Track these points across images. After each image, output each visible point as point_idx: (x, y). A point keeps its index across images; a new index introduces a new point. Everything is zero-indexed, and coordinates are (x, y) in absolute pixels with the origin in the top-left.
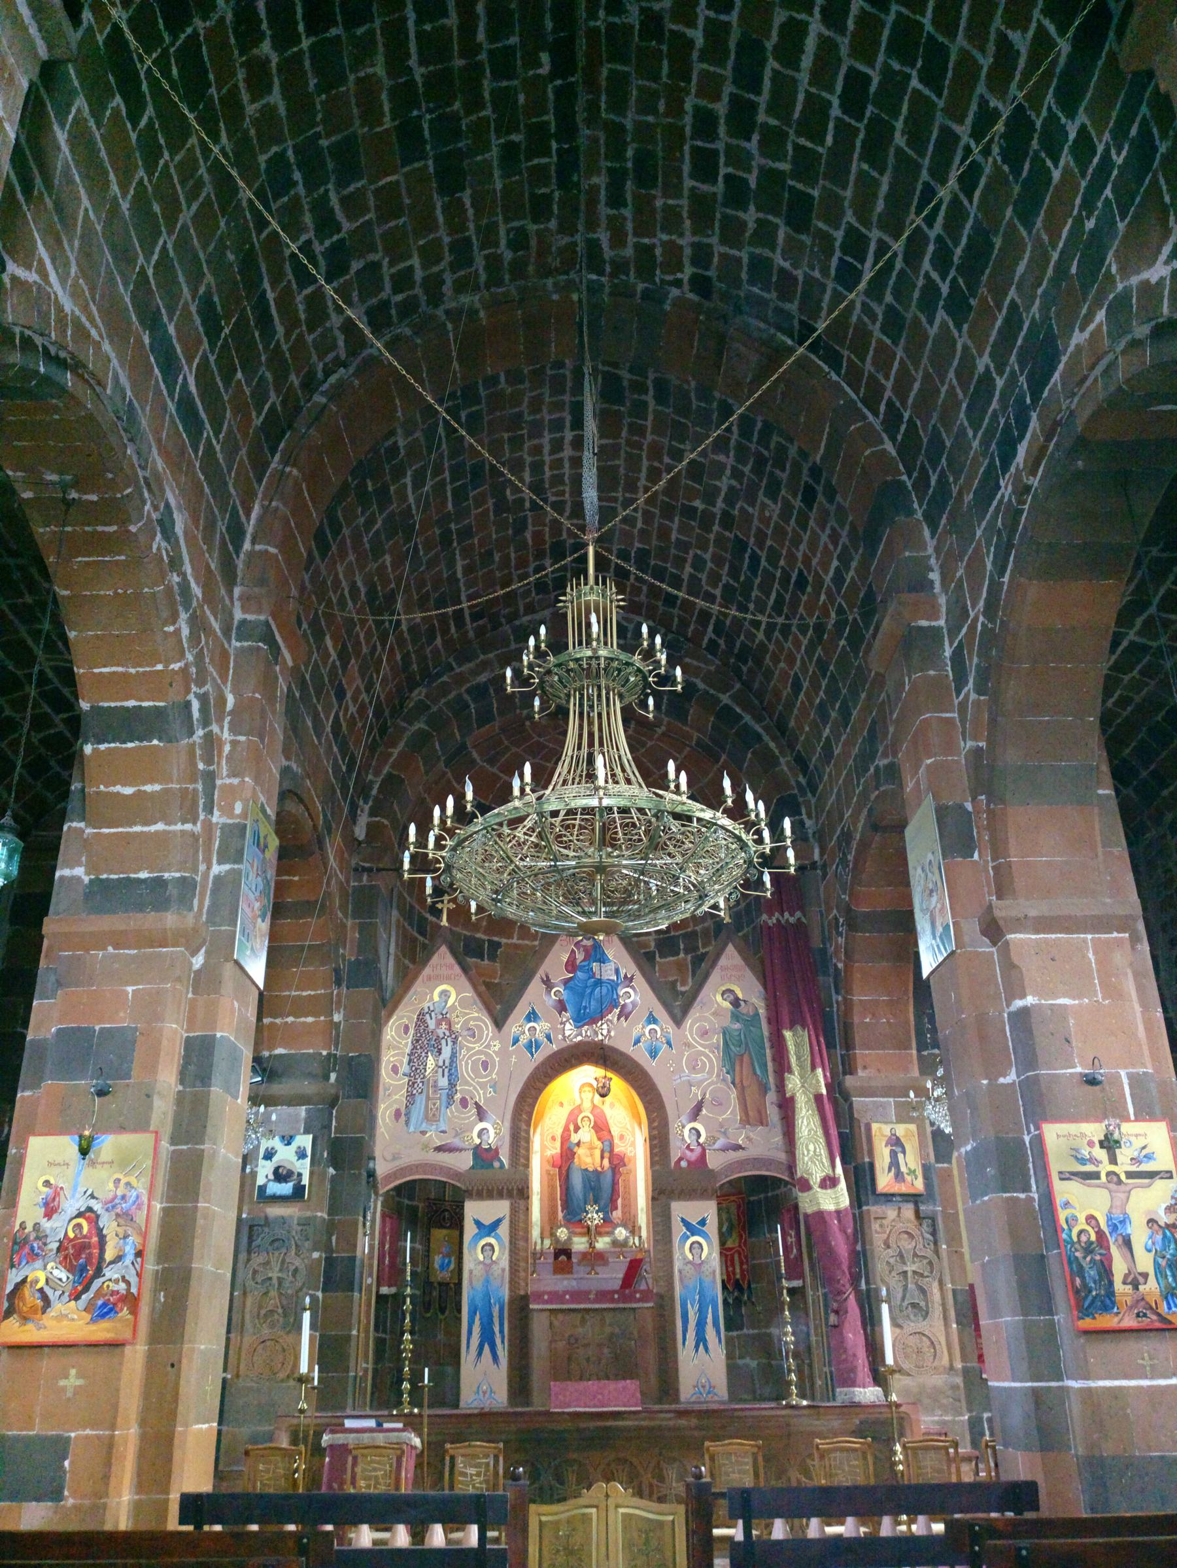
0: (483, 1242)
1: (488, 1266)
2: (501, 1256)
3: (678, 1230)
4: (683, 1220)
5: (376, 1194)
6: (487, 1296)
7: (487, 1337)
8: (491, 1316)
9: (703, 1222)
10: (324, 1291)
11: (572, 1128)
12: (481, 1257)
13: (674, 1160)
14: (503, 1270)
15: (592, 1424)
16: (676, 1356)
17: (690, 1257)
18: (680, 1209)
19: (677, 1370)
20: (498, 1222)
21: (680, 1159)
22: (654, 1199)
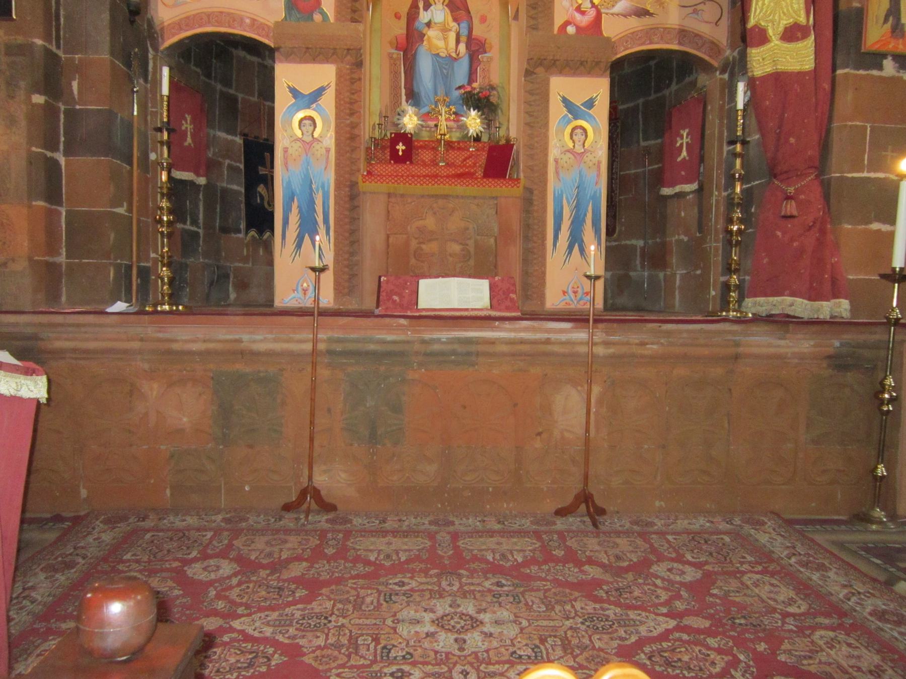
0: (301, 115)
1: (308, 145)
2: (325, 132)
3: (557, 111)
4: (565, 100)
5: (156, 49)
6: (308, 182)
7: (308, 227)
8: (312, 202)
9: (590, 104)
10: (67, 153)
11: (421, 5)
12: (299, 133)
13: (558, 22)
14: (328, 150)
15: (445, 335)
16: (544, 257)
17: (571, 145)
18: (561, 86)
19: (544, 273)
20: (320, 91)
21: (567, 23)
22: (528, 73)
